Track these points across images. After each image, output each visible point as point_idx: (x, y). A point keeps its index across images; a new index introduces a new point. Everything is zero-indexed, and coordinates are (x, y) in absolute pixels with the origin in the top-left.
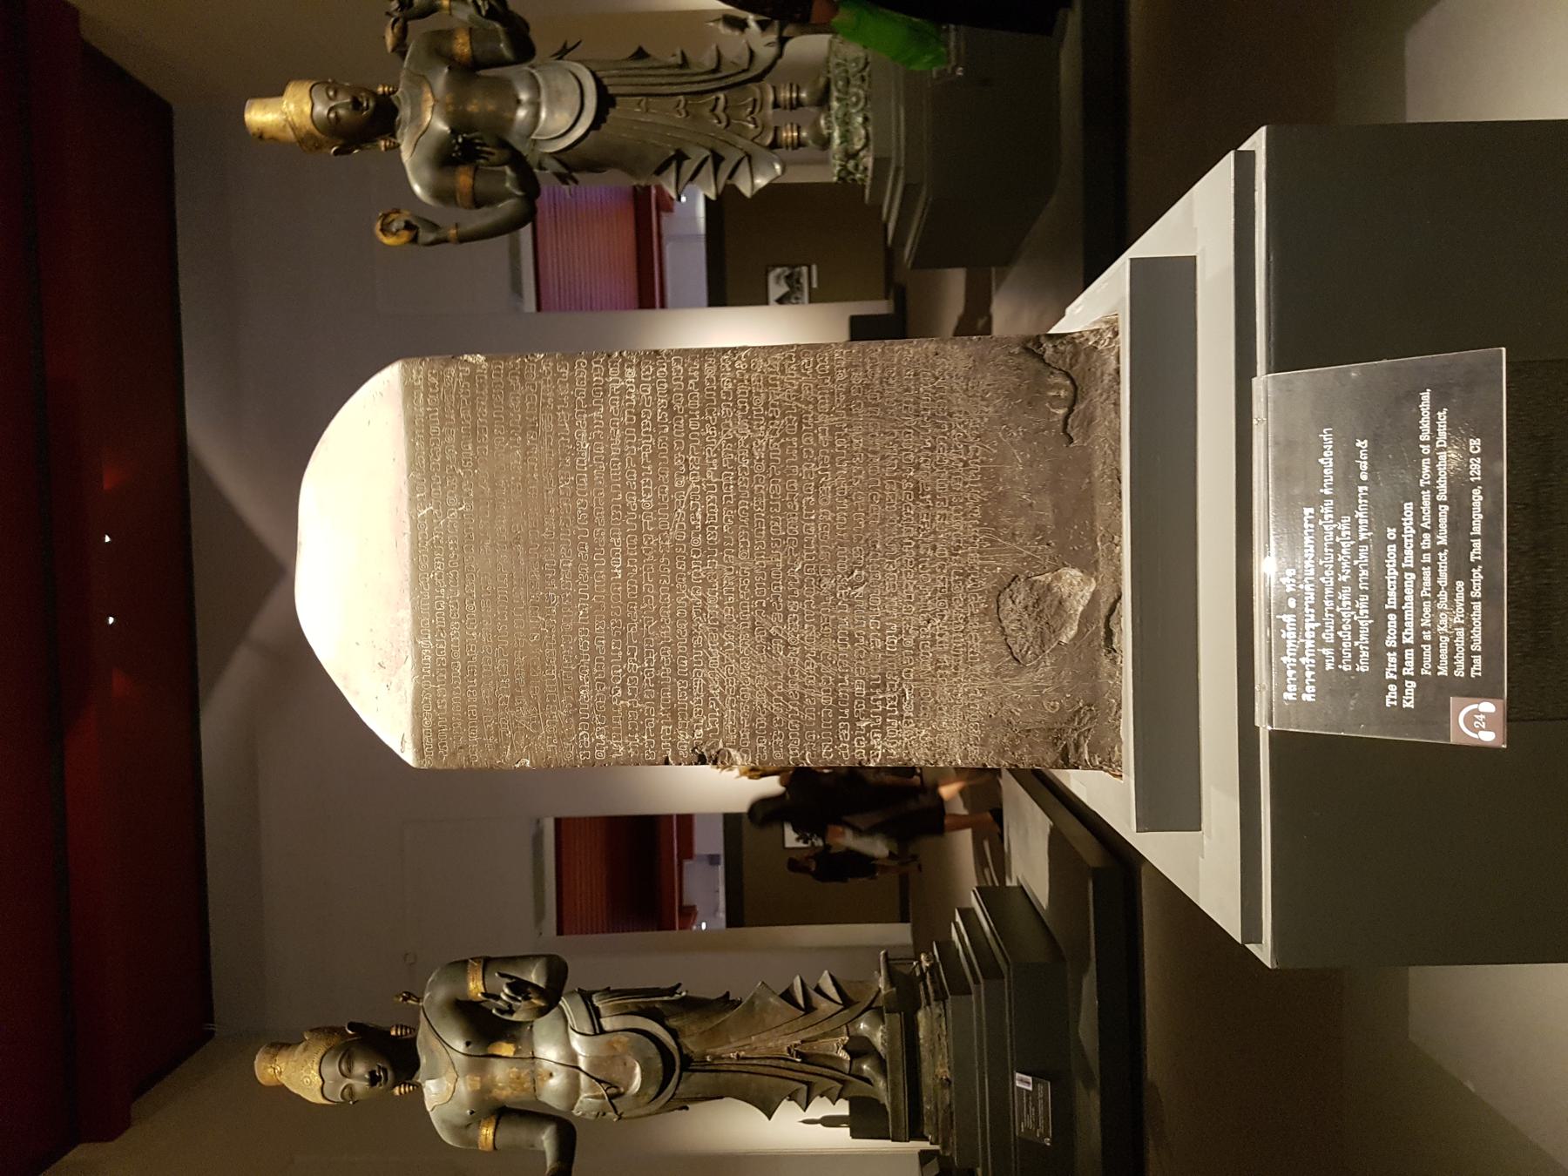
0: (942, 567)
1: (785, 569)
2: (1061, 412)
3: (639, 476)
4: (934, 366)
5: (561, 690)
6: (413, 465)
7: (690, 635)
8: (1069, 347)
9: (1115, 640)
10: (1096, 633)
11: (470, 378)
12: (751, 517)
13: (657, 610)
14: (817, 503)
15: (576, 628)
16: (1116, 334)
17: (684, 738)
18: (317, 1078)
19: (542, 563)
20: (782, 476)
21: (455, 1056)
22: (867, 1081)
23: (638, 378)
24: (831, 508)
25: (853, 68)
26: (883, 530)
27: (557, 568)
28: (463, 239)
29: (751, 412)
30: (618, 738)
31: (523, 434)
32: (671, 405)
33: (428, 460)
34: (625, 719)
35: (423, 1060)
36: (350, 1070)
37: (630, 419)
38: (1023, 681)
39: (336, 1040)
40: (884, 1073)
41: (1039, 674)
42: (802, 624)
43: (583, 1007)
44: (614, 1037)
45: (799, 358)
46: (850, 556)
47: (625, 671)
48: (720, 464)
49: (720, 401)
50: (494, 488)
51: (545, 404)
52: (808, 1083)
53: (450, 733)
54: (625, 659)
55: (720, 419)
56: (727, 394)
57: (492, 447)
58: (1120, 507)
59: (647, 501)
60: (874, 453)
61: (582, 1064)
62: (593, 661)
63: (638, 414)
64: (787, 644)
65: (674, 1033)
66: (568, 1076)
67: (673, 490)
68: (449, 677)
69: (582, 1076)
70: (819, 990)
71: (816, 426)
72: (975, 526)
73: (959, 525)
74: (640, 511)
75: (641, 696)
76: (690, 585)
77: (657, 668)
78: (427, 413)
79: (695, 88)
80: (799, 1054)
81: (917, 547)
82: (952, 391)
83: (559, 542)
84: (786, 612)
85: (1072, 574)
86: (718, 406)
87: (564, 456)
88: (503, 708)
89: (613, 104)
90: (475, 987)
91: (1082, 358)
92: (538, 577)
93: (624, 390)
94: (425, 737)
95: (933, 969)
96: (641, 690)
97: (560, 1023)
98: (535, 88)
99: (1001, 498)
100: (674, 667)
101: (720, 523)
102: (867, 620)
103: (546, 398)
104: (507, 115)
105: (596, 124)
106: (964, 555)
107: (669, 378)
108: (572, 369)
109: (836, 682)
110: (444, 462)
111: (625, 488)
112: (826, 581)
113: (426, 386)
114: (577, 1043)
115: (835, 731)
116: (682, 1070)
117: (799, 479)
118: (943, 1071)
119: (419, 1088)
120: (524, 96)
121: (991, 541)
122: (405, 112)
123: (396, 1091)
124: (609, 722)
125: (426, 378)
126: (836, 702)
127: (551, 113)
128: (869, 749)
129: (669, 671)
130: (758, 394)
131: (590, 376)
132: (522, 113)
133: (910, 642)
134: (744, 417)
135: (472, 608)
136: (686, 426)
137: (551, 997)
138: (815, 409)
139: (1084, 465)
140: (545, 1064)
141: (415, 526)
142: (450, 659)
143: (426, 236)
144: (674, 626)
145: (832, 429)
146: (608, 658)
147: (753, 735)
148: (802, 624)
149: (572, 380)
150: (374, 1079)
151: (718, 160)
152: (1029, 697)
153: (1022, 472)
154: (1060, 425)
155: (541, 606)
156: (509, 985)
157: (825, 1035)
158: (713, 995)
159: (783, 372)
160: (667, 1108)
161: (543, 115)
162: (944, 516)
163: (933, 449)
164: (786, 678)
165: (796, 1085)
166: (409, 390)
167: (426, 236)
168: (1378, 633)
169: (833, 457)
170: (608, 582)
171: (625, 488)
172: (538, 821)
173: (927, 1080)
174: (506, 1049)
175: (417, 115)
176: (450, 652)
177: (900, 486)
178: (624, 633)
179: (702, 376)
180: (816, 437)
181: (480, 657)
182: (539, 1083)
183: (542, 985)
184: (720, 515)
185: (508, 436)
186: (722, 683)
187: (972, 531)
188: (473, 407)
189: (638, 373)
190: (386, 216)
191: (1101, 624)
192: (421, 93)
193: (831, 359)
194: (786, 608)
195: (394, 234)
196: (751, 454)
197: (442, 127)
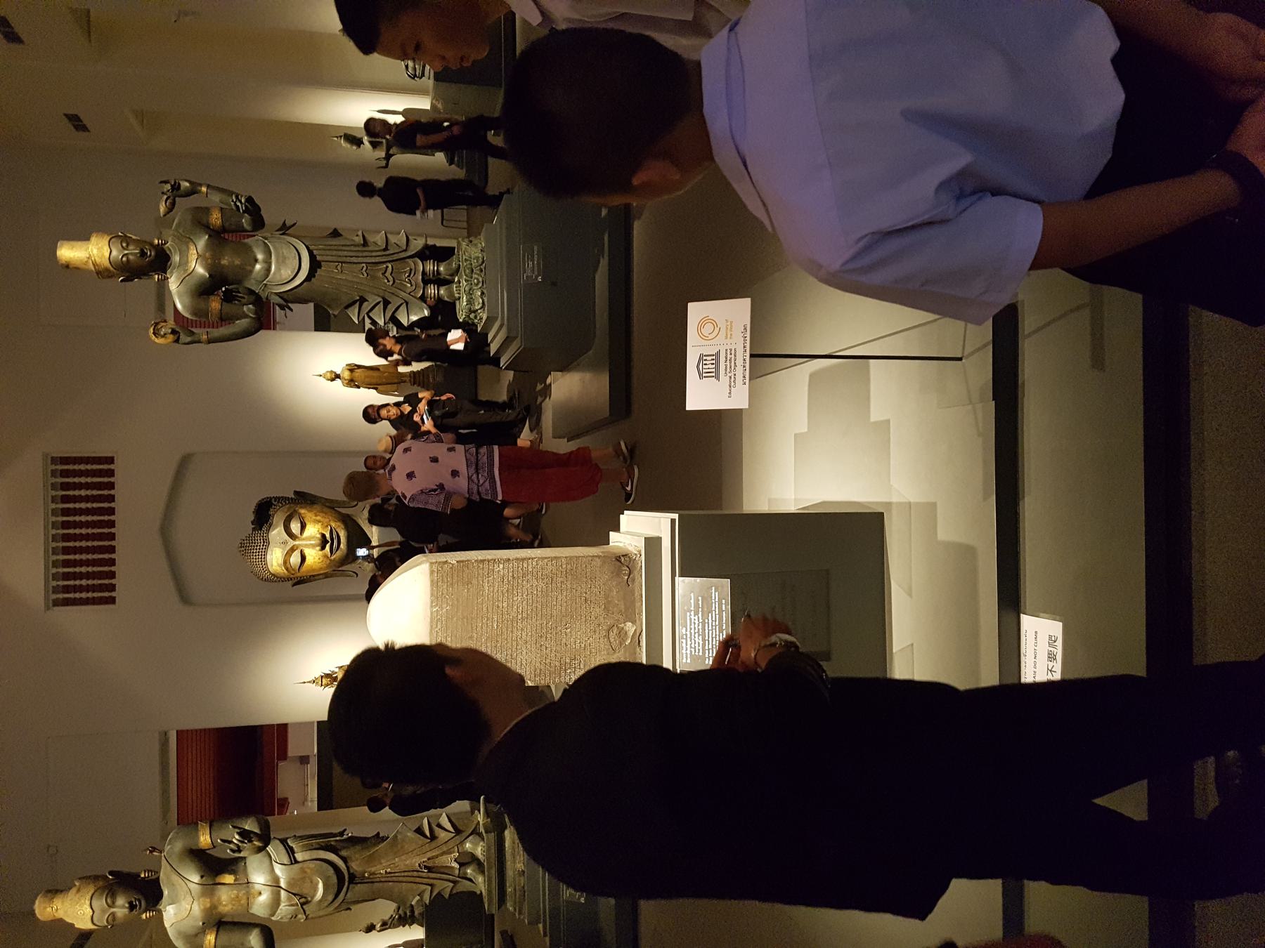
18: (89, 909)
21: (192, 886)
22: (470, 880)
25: (474, 263)
28: (209, 341)
35: (166, 893)
40: (483, 872)
43: (281, 847)
44: (305, 865)
52: (431, 885)
59: (505, 604)
61: (283, 884)
65: (344, 860)
66: (272, 892)
69: (283, 892)
70: (439, 826)
79: (373, 260)
80: (426, 867)
85: (629, 624)
89: (320, 267)
90: (204, 839)
97: (266, 860)
99: (609, 602)
104: (249, 268)
105: (308, 279)
114: (279, 870)
116: (350, 883)
118: (520, 866)
119: (160, 912)
120: (260, 257)
122: (176, 258)
123: (144, 916)
127: (278, 269)
132: (258, 267)
137: (265, 839)
140: (257, 887)
150: (132, 907)
151: (386, 303)
156: (239, 834)
157: (443, 853)
158: (369, 833)
160: (338, 910)
166: (432, 572)
168: (704, 645)
173: (510, 873)
174: (229, 879)
175: (184, 263)
182: (251, 900)
183: (257, 831)
190: (156, 324)
192: (188, 248)
195: (164, 336)
197: (200, 270)
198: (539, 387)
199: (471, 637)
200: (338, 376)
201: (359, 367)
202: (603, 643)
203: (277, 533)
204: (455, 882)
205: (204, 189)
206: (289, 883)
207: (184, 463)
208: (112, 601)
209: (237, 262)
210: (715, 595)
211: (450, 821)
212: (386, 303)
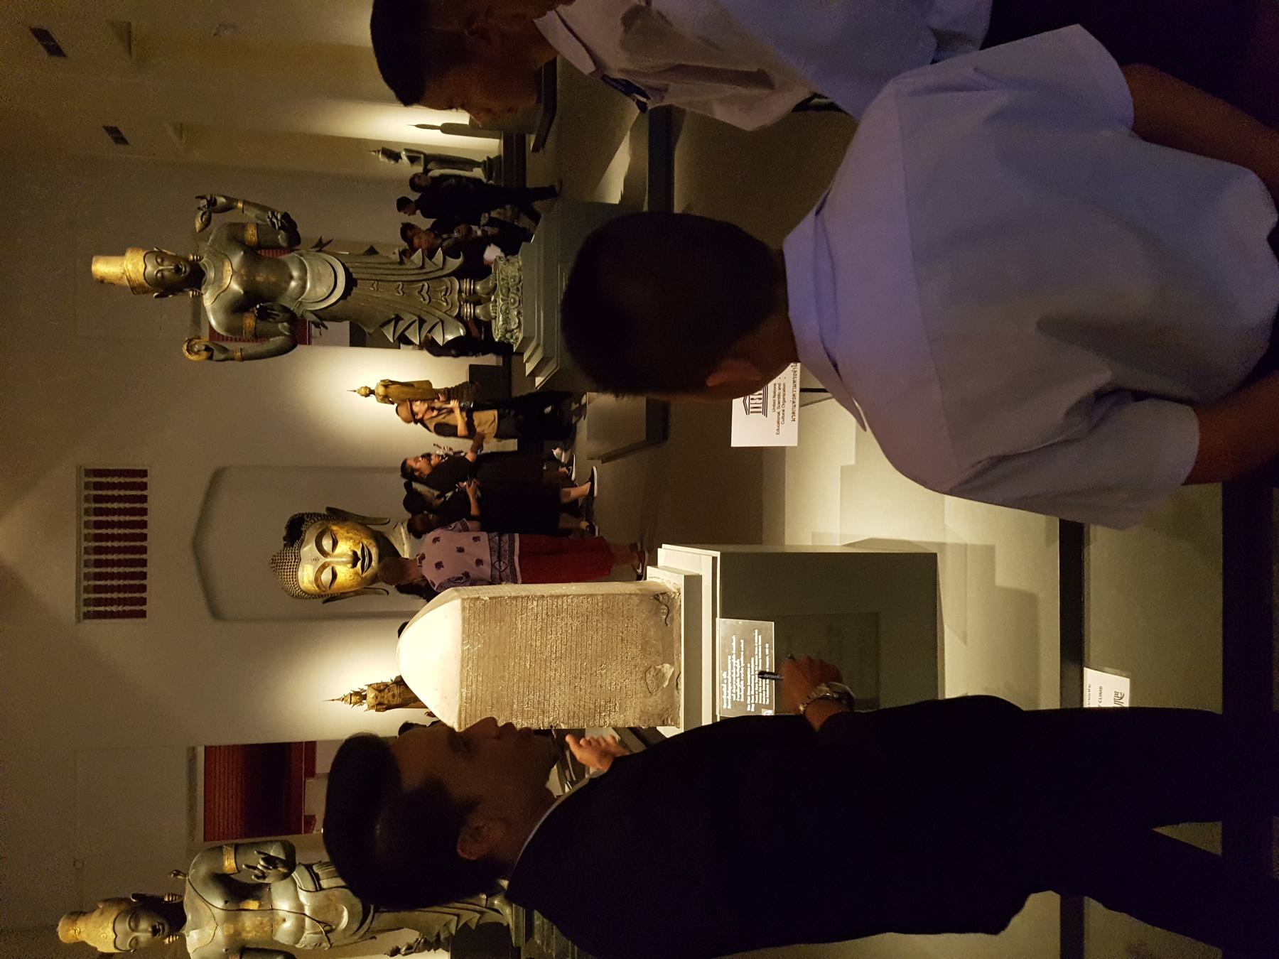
6: (463, 632)
21: (216, 911)
22: (497, 911)
25: (511, 282)
28: (243, 359)
35: (189, 917)
36: (137, 926)
38: (652, 699)
39: (123, 907)
43: (306, 874)
44: (330, 892)
52: (458, 916)
61: (307, 912)
66: (297, 919)
85: (667, 666)
90: (229, 864)
98: (303, 270)
99: (647, 643)
105: (344, 296)
114: (303, 897)
119: (183, 938)
120: (295, 274)
122: (211, 274)
123: (167, 941)
127: (314, 286)
132: (293, 284)
137: (290, 865)
139: (671, 632)
140: (282, 914)
141: (463, 652)
143: (218, 355)
150: (155, 931)
151: (422, 322)
161: (308, 285)
165: (448, 917)
166: (464, 609)
167: (218, 355)
168: (746, 691)
172: (194, 749)
174: (253, 905)
175: (219, 278)
183: (282, 856)
190: (190, 341)
195: (198, 353)
197: (235, 287)
198: (574, 406)
199: (503, 678)
200: (372, 392)
201: (394, 383)
202: (639, 686)
203: (309, 549)
204: (481, 913)
205: (240, 205)
206: (314, 911)
207: (217, 477)
208: (142, 614)
209: (273, 279)
210: (758, 639)
212: (422, 322)
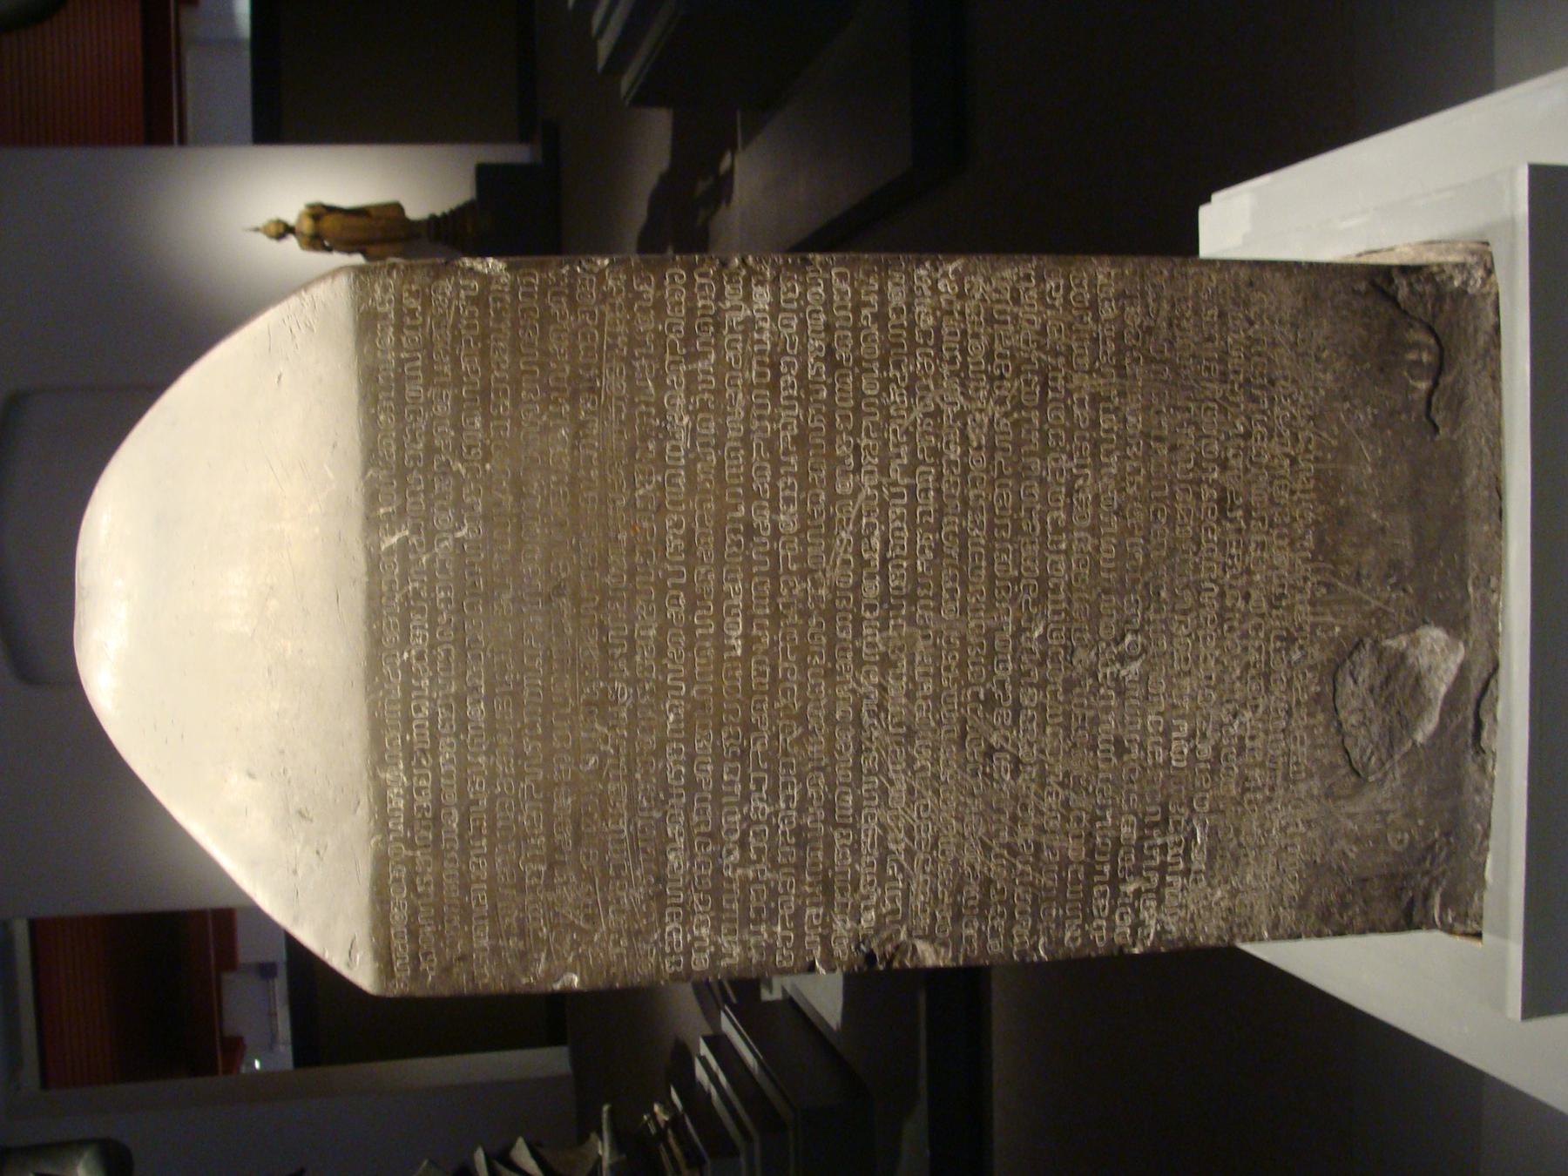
0: (1257, 628)
1: (1019, 631)
2: (1423, 385)
3: (776, 475)
4: (1247, 304)
5: (635, 854)
6: (371, 455)
7: (858, 752)
8: (1428, 288)
9: (1485, 734)
10: (1462, 726)
11: (479, 301)
12: (964, 547)
13: (804, 708)
14: (1069, 522)
15: (662, 743)
16: (1489, 271)
17: (842, 926)
19: (603, 630)
20: (1018, 477)
23: (776, 308)
24: (1094, 530)
26: (1172, 568)
27: (631, 639)
29: (965, 365)
30: (732, 932)
31: (574, 399)
32: (831, 351)
33: (401, 447)
34: (744, 902)
37: (761, 375)
38: (1360, 806)
41: (1385, 793)
42: (1043, 726)
45: (1041, 279)
46: (1120, 610)
47: (746, 818)
48: (913, 453)
49: (913, 344)
50: (519, 495)
51: (611, 347)
53: (440, 935)
54: (746, 797)
55: (914, 377)
56: (926, 334)
57: (517, 423)
58: (1499, 533)
59: (788, 519)
60: (1159, 439)
62: (690, 802)
63: (775, 366)
64: (1017, 761)
67: (833, 497)
68: (437, 838)
71: (1069, 393)
72: (1306, 560)
73: (1282, 559)
74: (776, 534)
75: (773, 860)
76: (859, 663)
77: (801, 810)
78: (401, 363)
81: (1222, 594)
82: (1274, 344)
83: (634, 593)
84: (1017, 708)
85: (1434, 636)
86: (912, 354)
87: (644, 438)
88: (533, 889)
91: (1447, 307)
92: (596, 654)
93: (749, 323)
94: (396, 943)
95: (676, 1123)
96: (773, 848)
100: (830, 807)
101: (912, 556)
102: (1144, 716)
103: (614, 336)
106: (1290, 608)
107: (828, 304)
108: (660, 286)
109: (1092, 821)
110: (431, 450)
111: (751, 496)
112: (1080, 654)
113: (400, 314)
115: (1087, 899)
117: (1042, 481)
121: (1328, 586)
124: (718, 906)
125: (399, 301)
126: (1090, 854)
128: (1138, 924)
129: (822, 814)
130: (976, 336)
131: (691, 298)
133: (1206, 750)
134: (954, 374)
135: (477, 712)
136: (857, 388)
138: (1069, 364)
139: (1453, 464)
141: (374, 563)
142: (438, 804)
144: (831, 738)
145: (1095, 399)
146: (717, 792)
147: (957, 917)
148: (1043, 726)
149: (659, 305)
152: (1370, 828)
153: (1372, 477)
154: (1422, 406)
155: (601, 706)
159: (1016, 300)
162: (1261, 546)
163: (1247, 436)
164: (1014, 819)
166: (366, 323)
169: (1096, 445)
170: (719, 660)
171: (751, 496)
176: (437, 791)
177: (1198, 496)
178: (745, 752)
179: (884, 302)
180: (1069, 410)
181: (492, 800)
184: (912, 542)
185: (546, 402)
186: (909, 832)
187: (1302, 569)
188: (484, 354)
189: (775, 294)
191: (1470, 712)
193: (1093, 283)
194: (1017, 701)
196: (965, 439)
199: (601, 706)
211: (536, 1155)
